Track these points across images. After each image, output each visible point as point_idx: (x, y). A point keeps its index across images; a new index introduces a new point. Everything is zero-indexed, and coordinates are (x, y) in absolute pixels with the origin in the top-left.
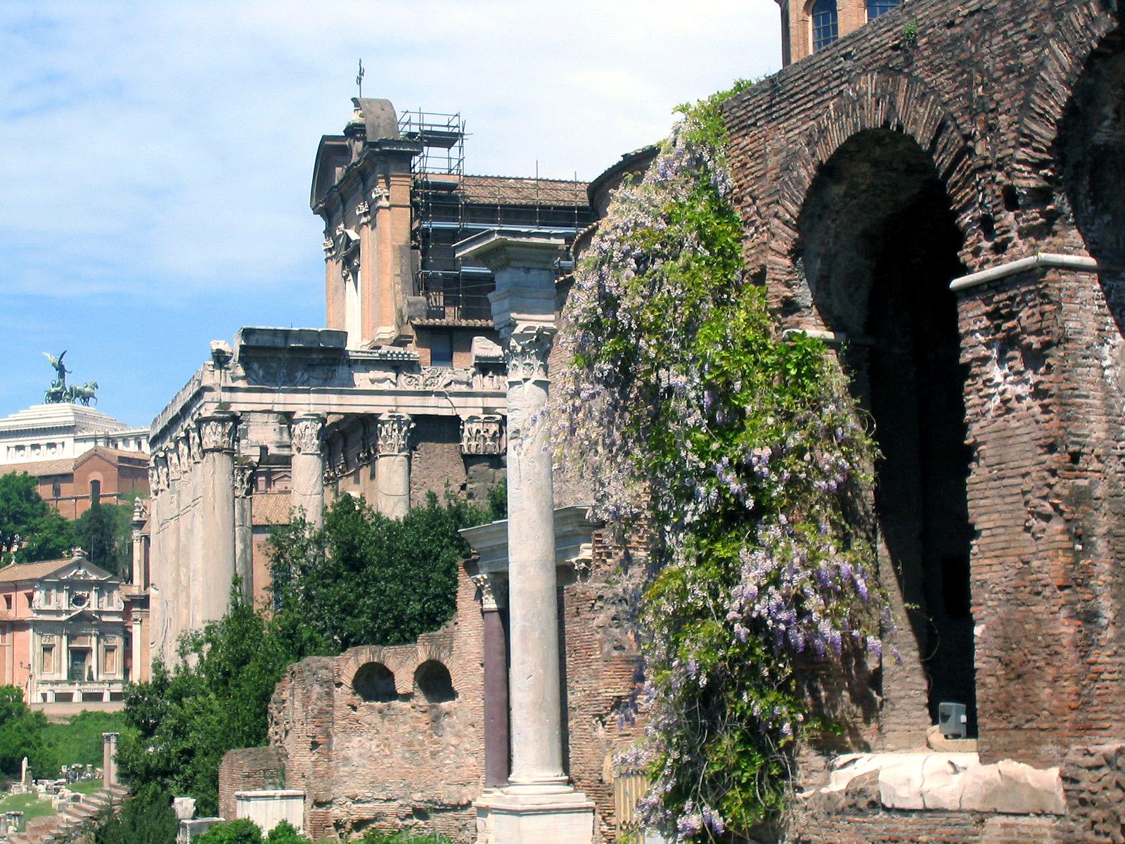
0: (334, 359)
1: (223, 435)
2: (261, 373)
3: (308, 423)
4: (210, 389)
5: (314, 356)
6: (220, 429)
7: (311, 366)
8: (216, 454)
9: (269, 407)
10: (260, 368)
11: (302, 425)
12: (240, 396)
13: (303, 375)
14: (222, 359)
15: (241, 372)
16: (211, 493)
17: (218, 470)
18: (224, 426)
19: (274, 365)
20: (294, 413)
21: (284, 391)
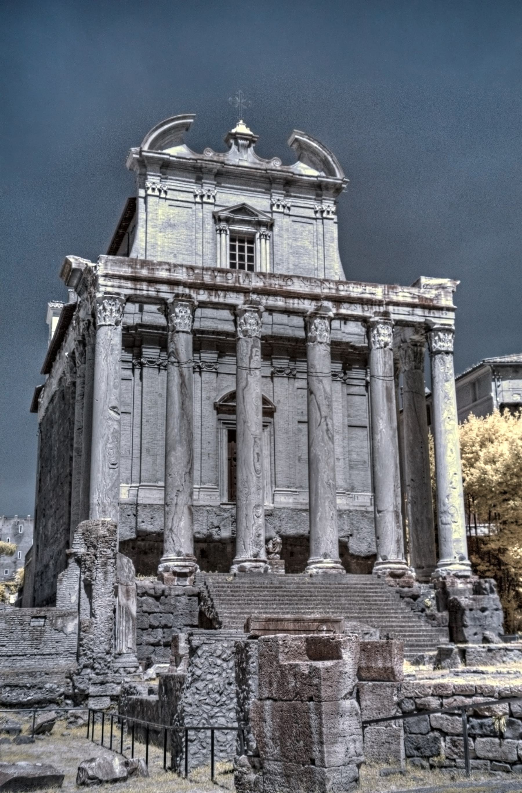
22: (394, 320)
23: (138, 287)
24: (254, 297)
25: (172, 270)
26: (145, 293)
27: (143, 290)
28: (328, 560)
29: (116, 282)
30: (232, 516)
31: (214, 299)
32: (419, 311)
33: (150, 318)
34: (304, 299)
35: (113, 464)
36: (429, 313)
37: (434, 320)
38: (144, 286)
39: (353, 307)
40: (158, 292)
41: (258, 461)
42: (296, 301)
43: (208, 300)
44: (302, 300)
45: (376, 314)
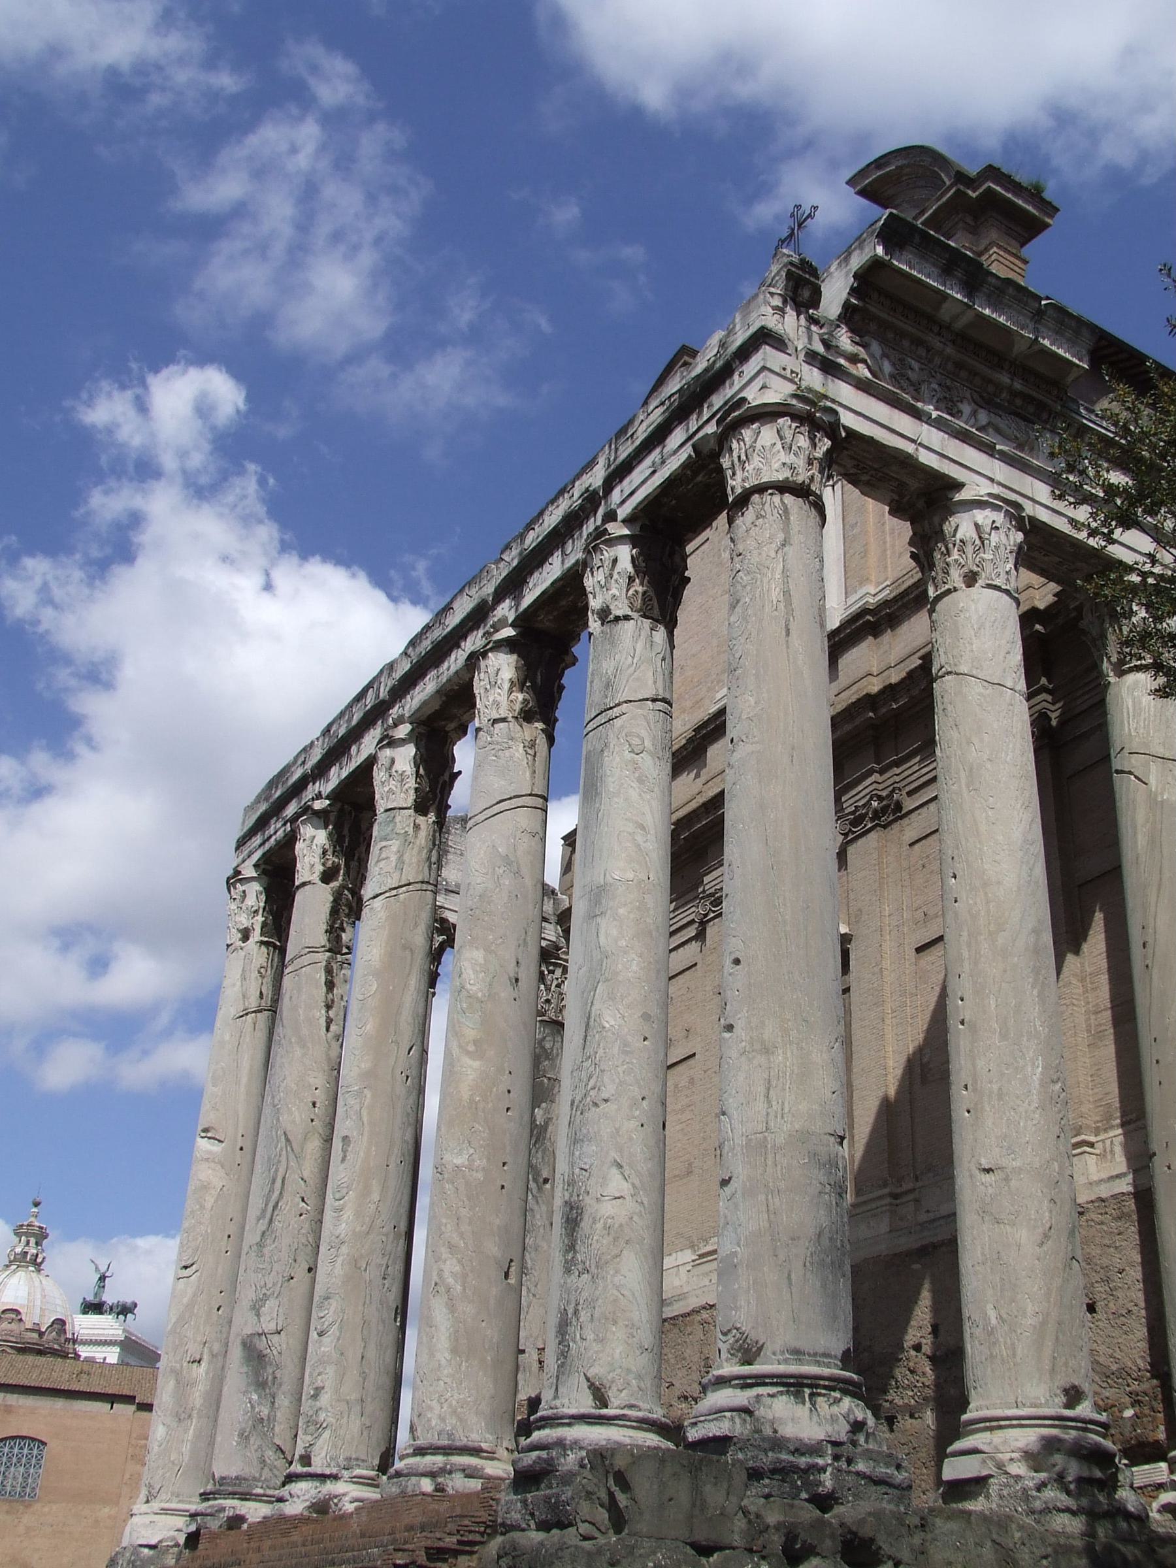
0: (1041, 406)
1: (810, 462)
2: (887, 367)
3: (999, 518)
4: (779, 342)
5: (1005, 379)
6: (803, 441)
7: (987, 401)
8: (788, 498)
9: (910, 448)
10: (885, 355)
11: (983, 517)
12: (844, 392)
13: (974, 413)
14: (806, 294)
15: (844, 339)
16: (775, 593)
17: (796, 539)
18: (812, 439)
19: (916, 365)
20: (959, 486)
21: (939, 424)
23: (267, 834)
24: (395, 712)
31: (345, 774)
32: (677, 437)
36: (700, 414)
39: (546, 567)
41: (343, 1160)
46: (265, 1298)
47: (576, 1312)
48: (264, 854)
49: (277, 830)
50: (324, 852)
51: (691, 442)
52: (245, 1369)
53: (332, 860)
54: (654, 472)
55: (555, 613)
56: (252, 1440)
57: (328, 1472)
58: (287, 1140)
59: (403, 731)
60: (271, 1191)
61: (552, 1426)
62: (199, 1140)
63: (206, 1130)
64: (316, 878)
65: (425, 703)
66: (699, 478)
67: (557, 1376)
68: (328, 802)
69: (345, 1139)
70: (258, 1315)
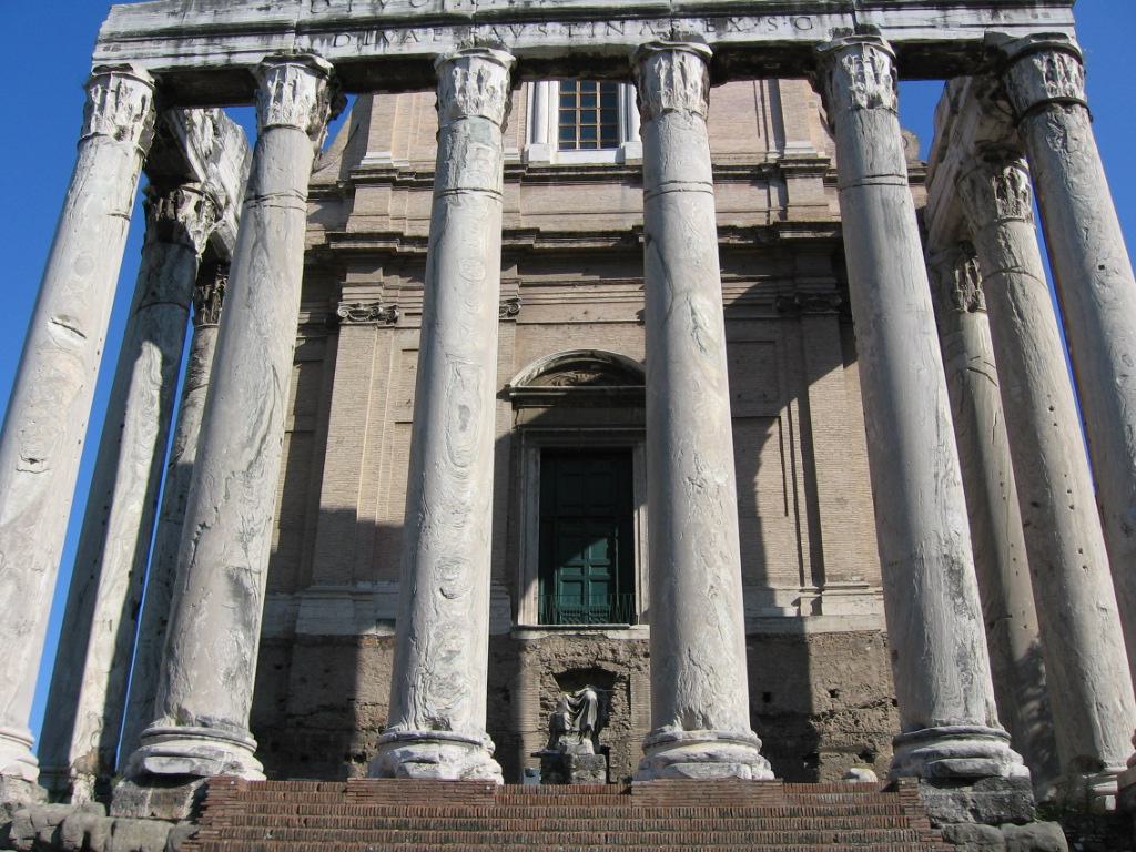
22: (894, 44)
23: (183, 49)
24: (484, 32)
25: (272, 9)
26: (197, 61)
27: (194, 55)
28: (697, 735)
29: (128, 50)
30: (542, 661)
31: (372, 49)
33: (365, 226)
34: (623, 20)
35: (33, 461)
37: (1009, 32)
38: (199, 45)
40: (230, 54)
42: (600, 28)
43: (356, 54)
44: (617, 24)
45: (836, 33)
46: (252, 533)
47: (972, 647)
48: (174, 68)
49: (202, 54)
50: (313, 108)
51: (984, 29)
52: (231, 603)
53: (317, 121)
54: (934, 27)
55: (743, 59)
56: (238, 682)
57: (477, 740)
58: (275, 375)
59: (506, 57)
60: (259, 421)
61: (978, 739)
62: (50, 324)
63: (64, 317)
64: (304, 127)
65: (544, 48)
66: (960, 54)
67: (966, 699)
68: (329, 66)
69: (463, 408)
70: (246, 549)
